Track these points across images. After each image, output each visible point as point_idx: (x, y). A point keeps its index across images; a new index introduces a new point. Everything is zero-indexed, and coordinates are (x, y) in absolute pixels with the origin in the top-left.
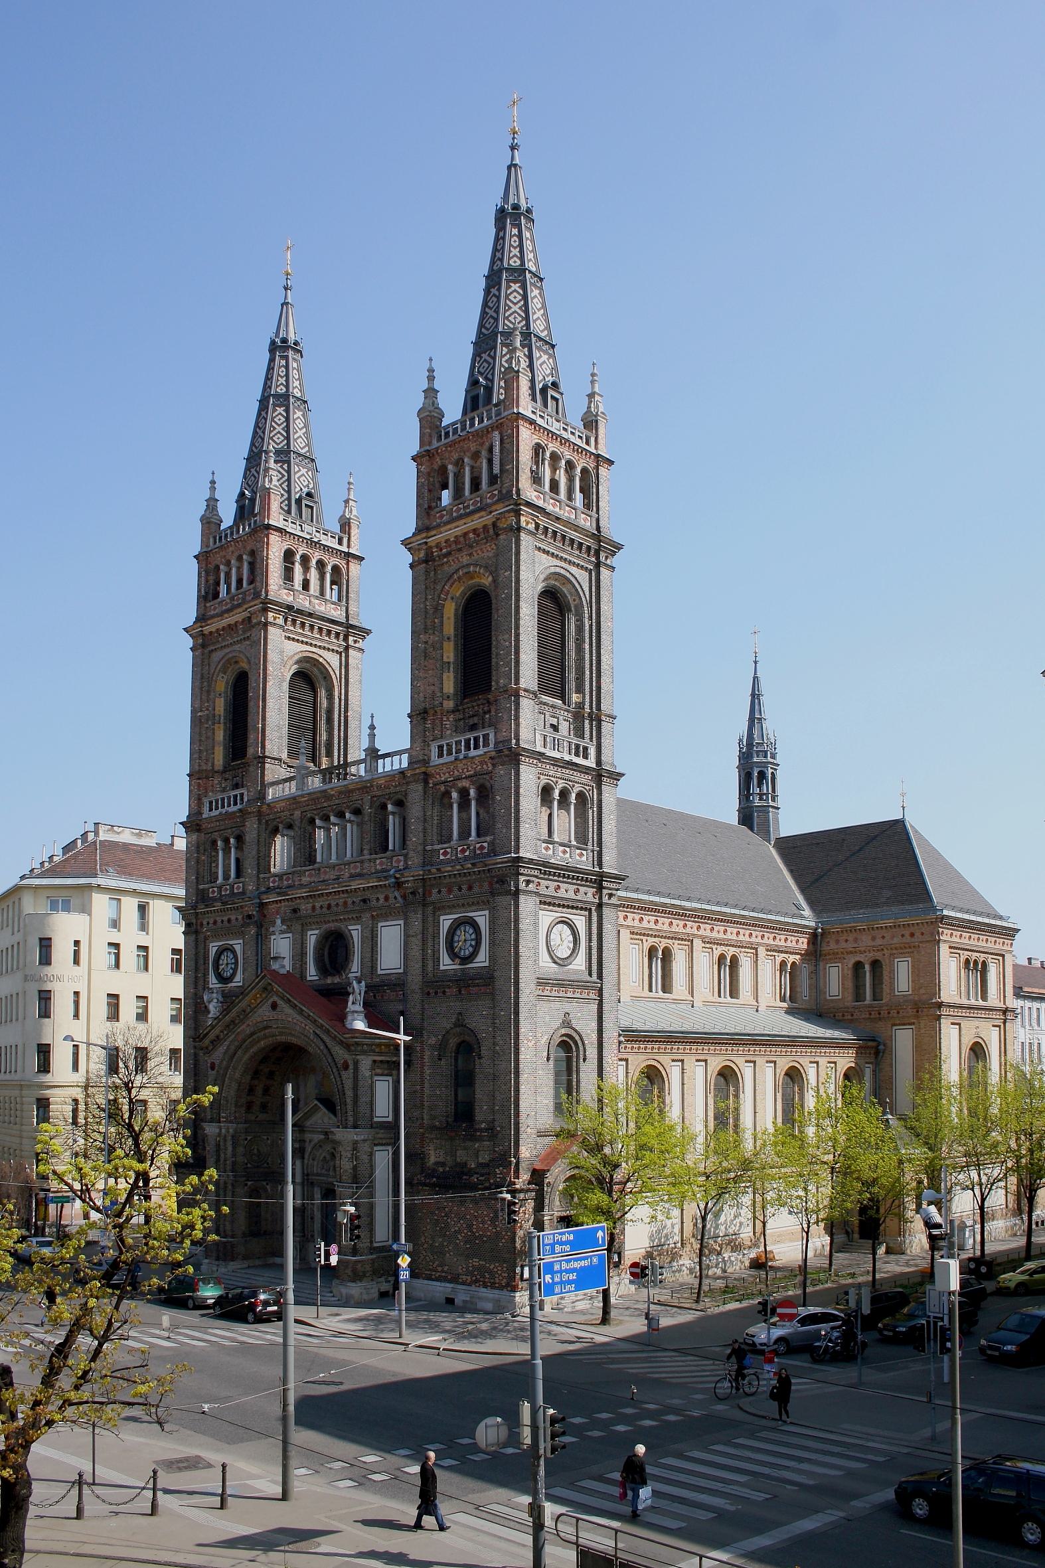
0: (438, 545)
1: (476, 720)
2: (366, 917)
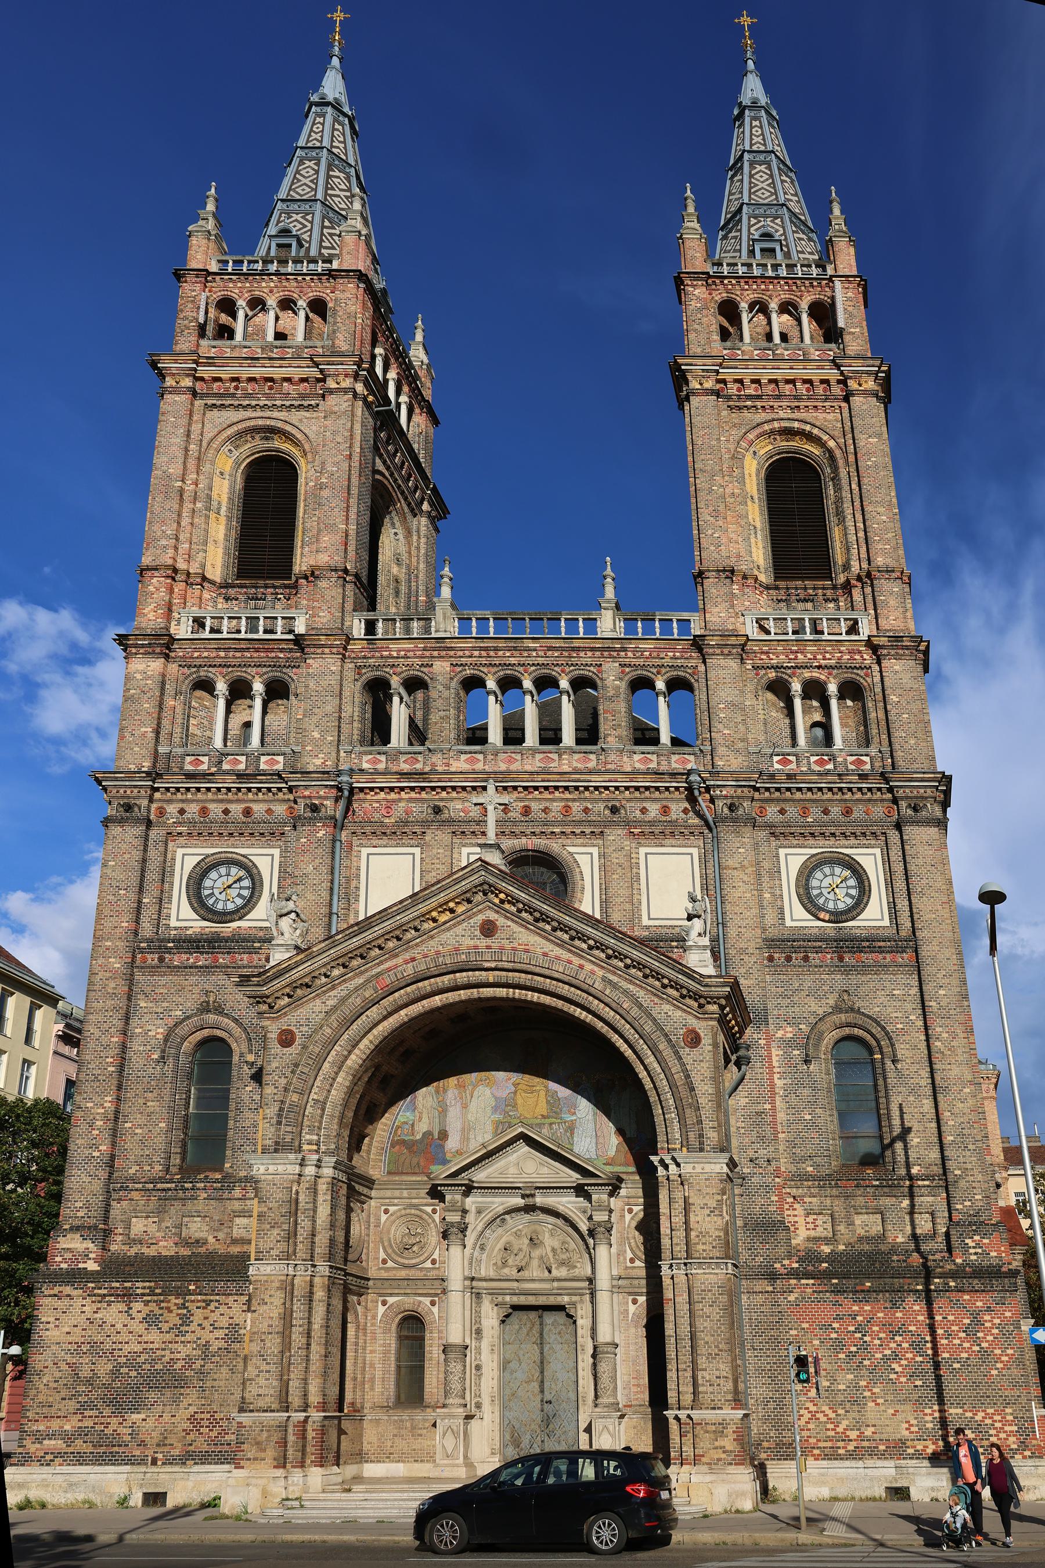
2: (615, 835)
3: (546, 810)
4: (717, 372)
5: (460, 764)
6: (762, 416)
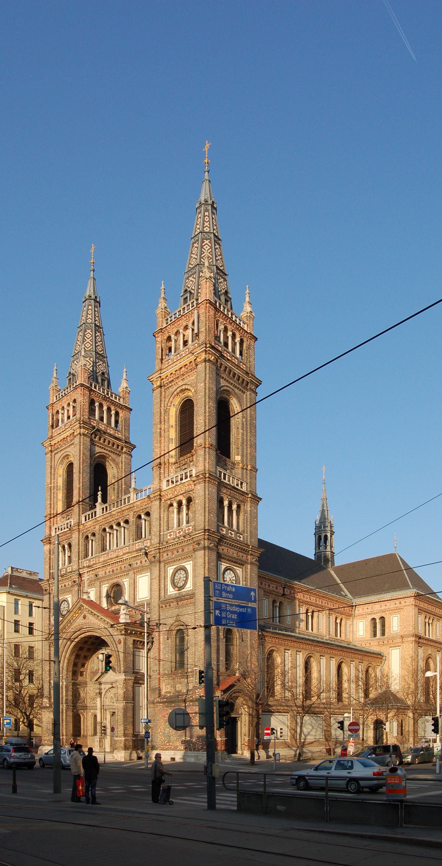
3: (117, 569)
4: (160, 377)
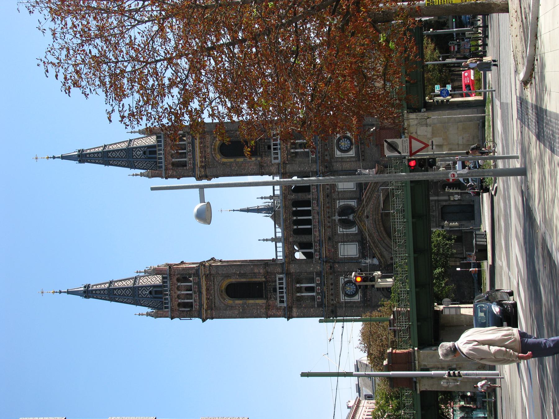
0: (202, 162)
1: (266, 147)
2: (334, 196)
3: (329, 212)
5: (317, 234)
6: (210, 157)
